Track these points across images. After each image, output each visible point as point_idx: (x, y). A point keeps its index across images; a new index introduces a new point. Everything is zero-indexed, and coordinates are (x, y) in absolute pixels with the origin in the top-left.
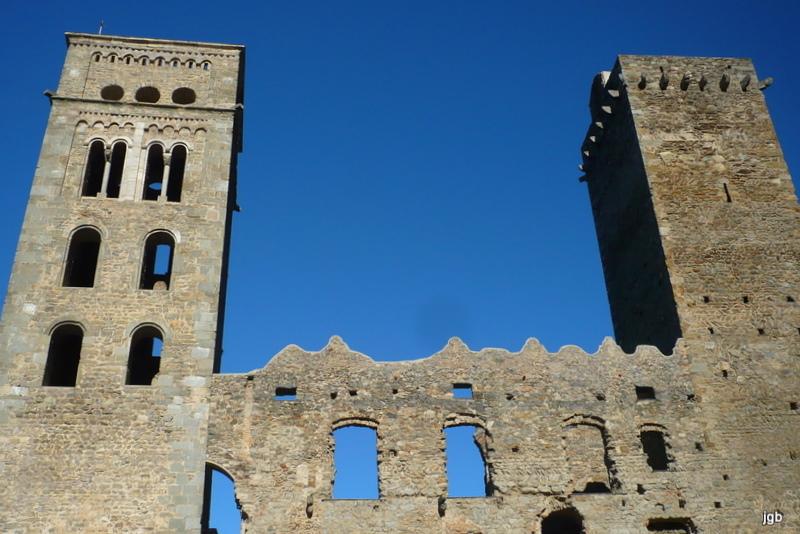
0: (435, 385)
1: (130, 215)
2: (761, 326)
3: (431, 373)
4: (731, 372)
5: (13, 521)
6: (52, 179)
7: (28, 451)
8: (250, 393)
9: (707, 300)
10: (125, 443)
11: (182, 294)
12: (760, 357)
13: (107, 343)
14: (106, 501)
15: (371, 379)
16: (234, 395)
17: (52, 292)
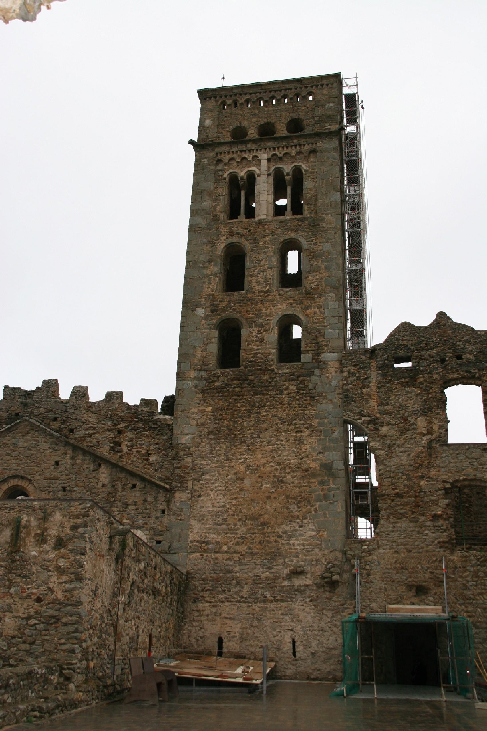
5: (208, 468)
6: (203, 210)
7: (212, 418)
10: (281, 408)
11: (312, 289)
13: (259, 332)
14: (272, 451)
15: (474, 345)
16: (362, 366)
17: (214, 298)
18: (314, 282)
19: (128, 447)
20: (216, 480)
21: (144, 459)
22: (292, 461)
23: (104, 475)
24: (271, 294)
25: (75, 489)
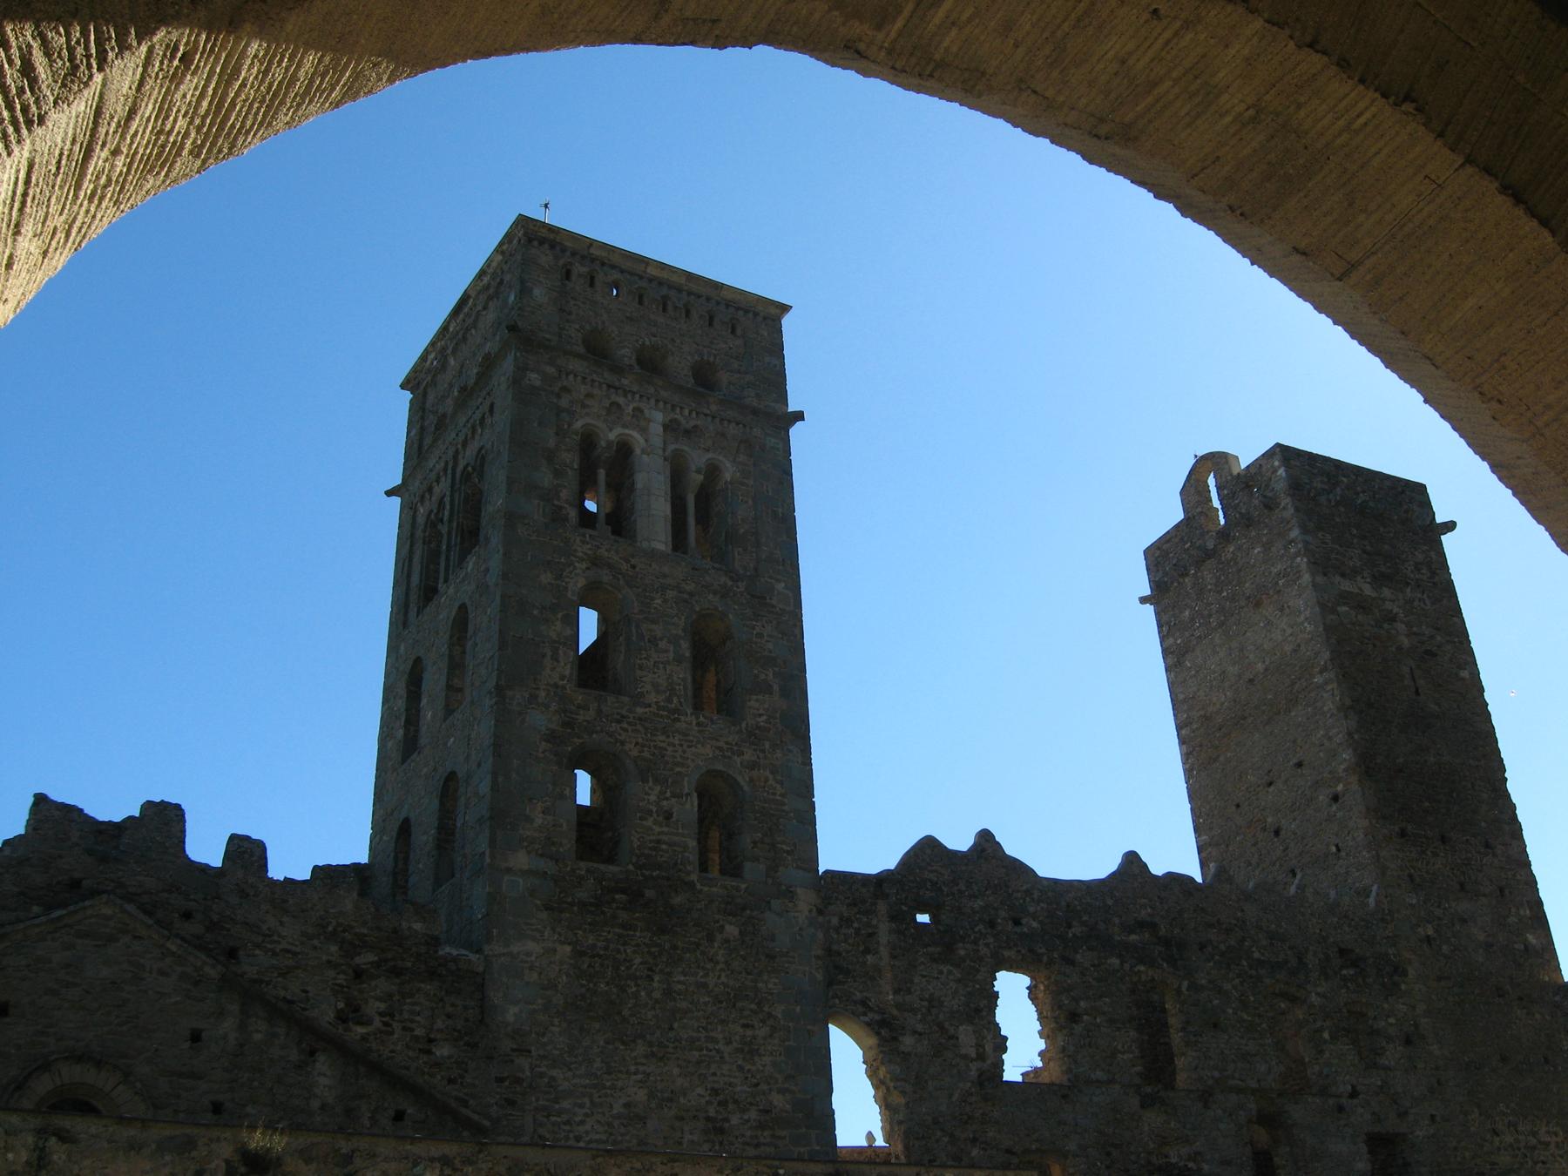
0: (1117, 920)
1: (665, 576)
3: (1110, 902)
8: (882, 907)
9: (1403, 834)
12: (1464, 921)
18: (760, 715)
19: (381, 1014)
20: (586, 1115)
21: (420, 1050)
22: (739, 1089)
23: (323, 1081)
24: (683, 718)
25: (249, 1109)
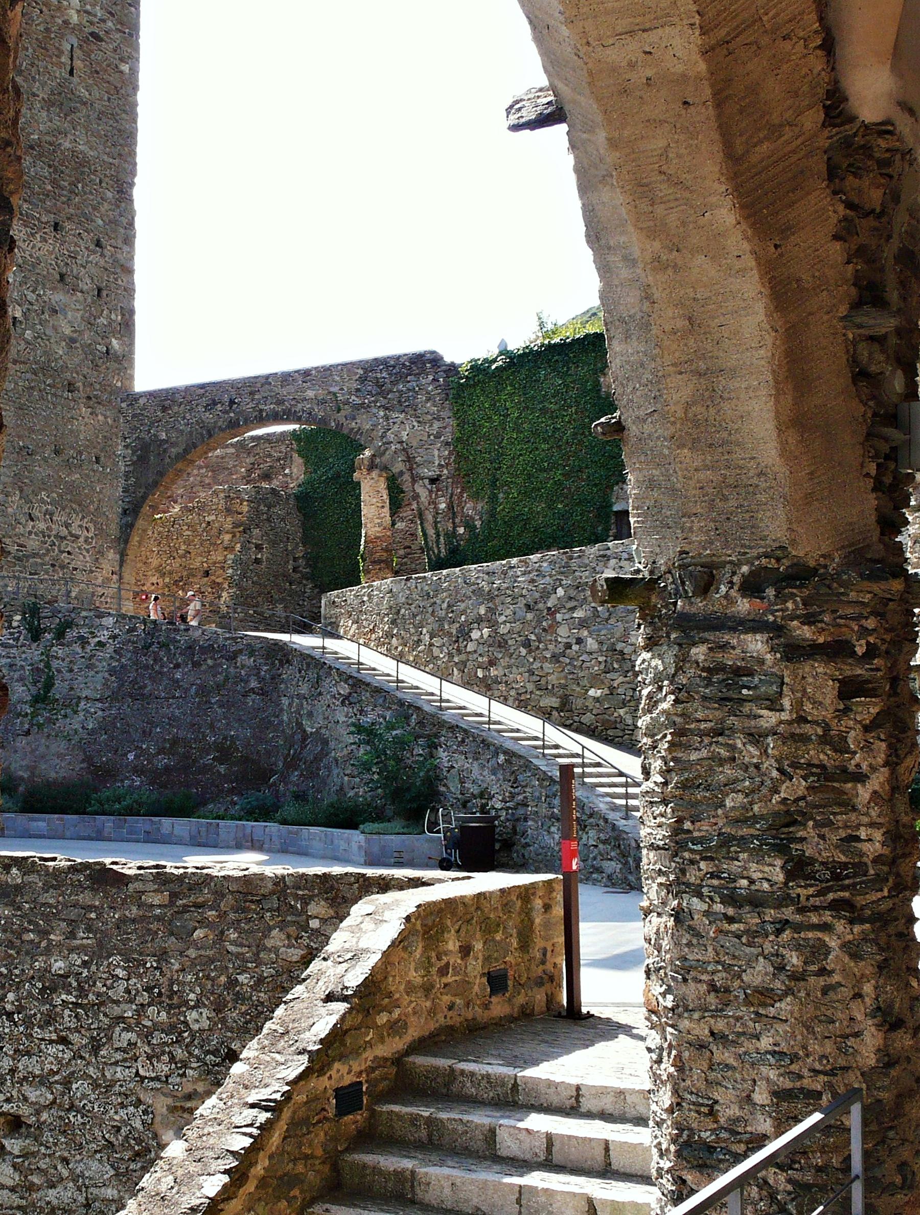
2: (64, 270)
4: (21, 322)
